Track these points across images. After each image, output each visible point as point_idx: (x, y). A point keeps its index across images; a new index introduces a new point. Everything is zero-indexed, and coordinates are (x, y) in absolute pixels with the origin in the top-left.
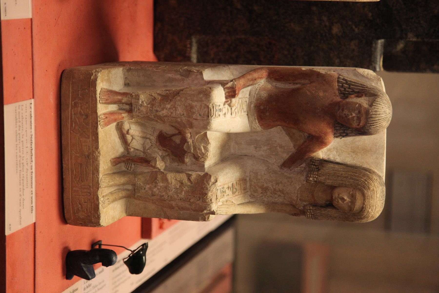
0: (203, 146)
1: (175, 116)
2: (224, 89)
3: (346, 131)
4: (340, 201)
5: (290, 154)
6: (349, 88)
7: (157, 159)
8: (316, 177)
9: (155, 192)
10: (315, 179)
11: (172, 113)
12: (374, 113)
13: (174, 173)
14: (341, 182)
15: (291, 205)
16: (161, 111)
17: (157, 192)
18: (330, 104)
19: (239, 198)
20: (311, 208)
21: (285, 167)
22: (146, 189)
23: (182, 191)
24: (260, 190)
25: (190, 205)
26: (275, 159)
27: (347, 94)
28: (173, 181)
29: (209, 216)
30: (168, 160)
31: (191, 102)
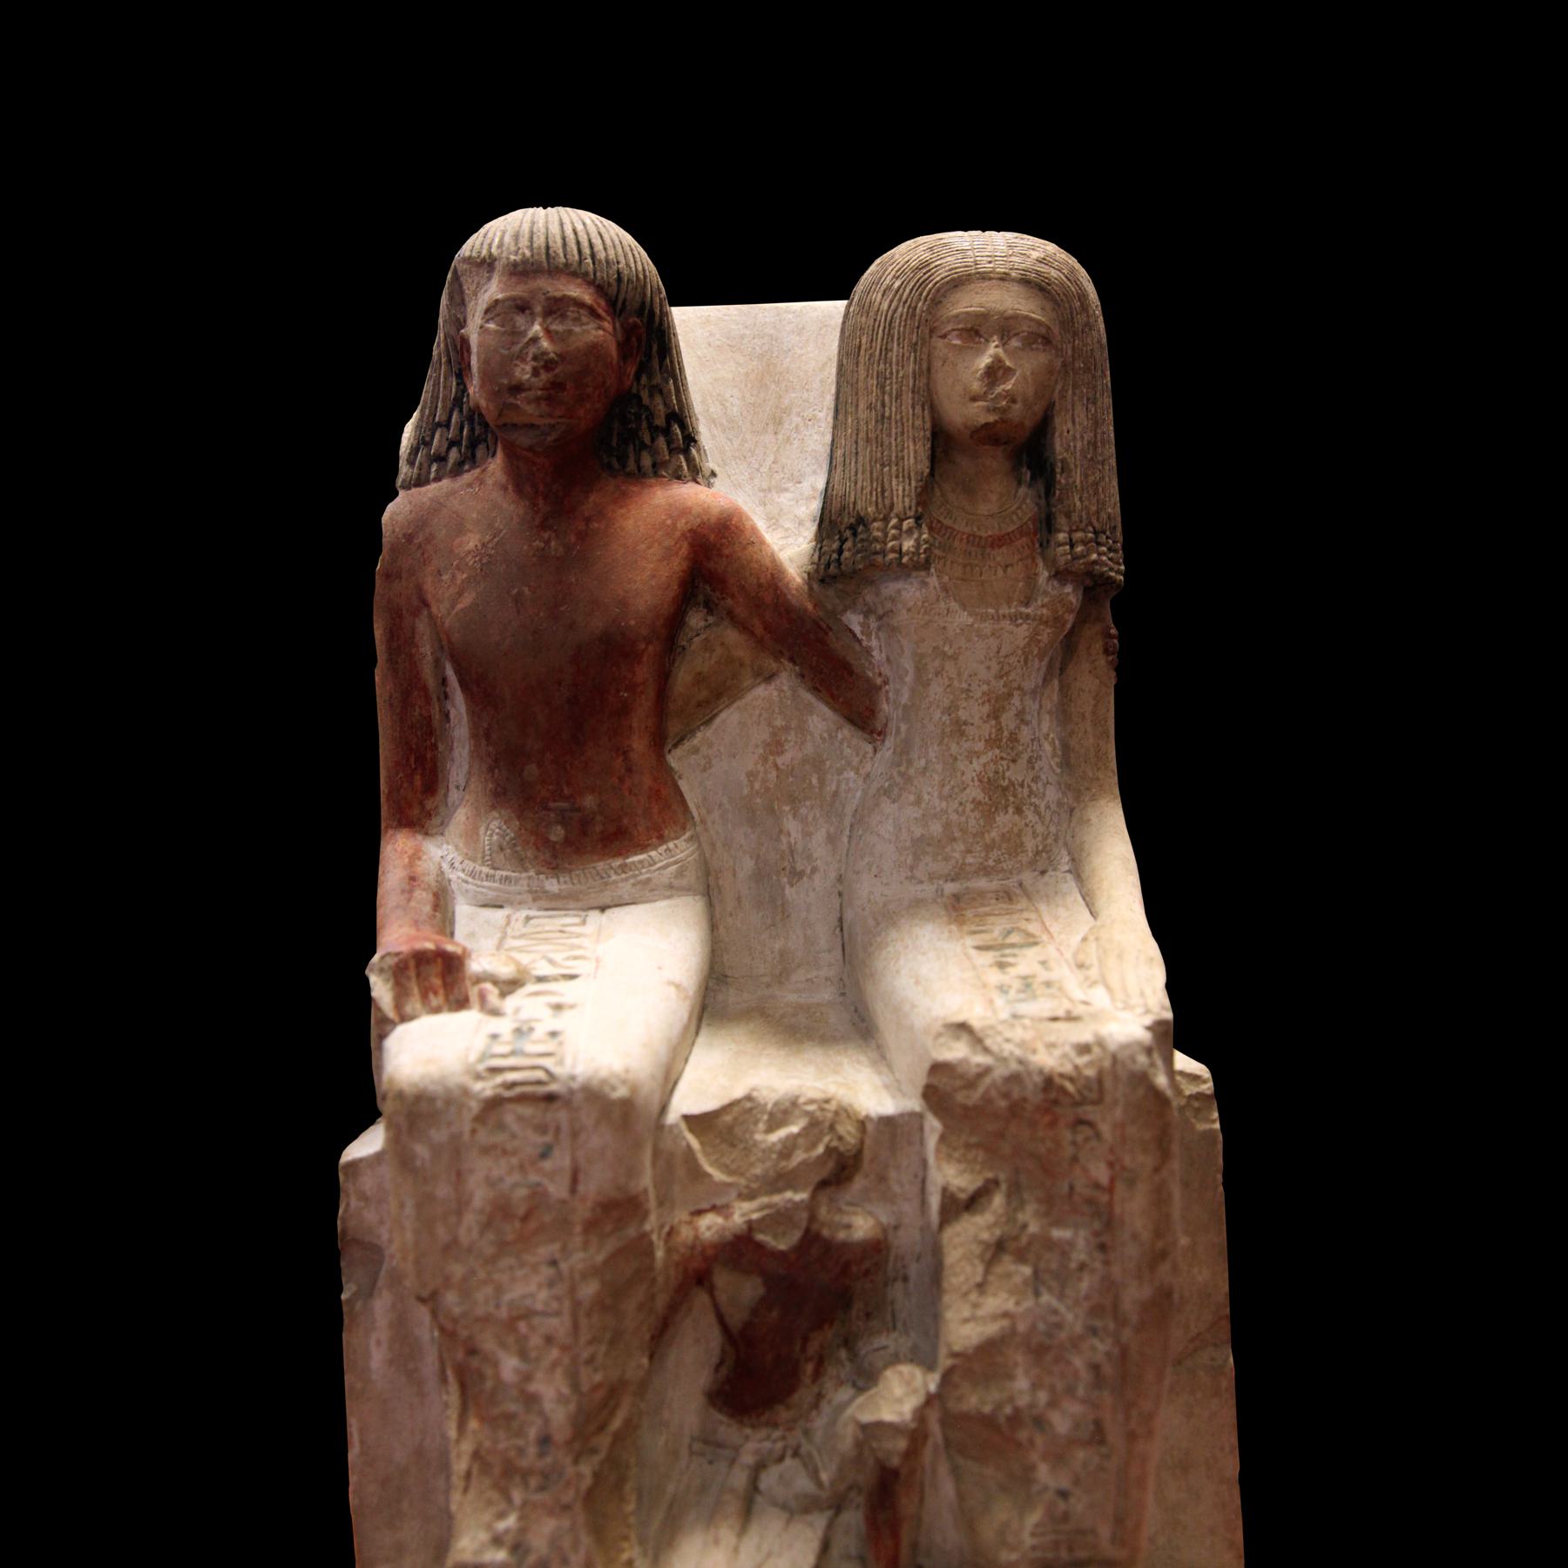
0: (770, 1129)
1: (567, 1318)
2: (404, 1018)
3: (660, 421)
4: (1008, 386)
5: (808, 697)
6: (447, 425)
7: (867, 1417)
8: (894, 521)
9: (1077, 1426)
10: (905, 525)
11: (549, 1340)
12: (524, 242)
13: (946, 1299)
14: (908, 398)
15: (1062, 670)
16: (541, 1413)
17: (1075, 1408)
18: (519, 490)
19: (1056, 918)
20: (1062, 536)
21: (872, 712)
22: (1065, 1484)
23: (1050, 1244)
24: (1005, 820)
25: (1131, 1183)
26: (840, 772)
27: (472, 430)
28: (996, 1302)
29: (1182, 1073)
30: (882, 1340)
31: (470, 1219)
